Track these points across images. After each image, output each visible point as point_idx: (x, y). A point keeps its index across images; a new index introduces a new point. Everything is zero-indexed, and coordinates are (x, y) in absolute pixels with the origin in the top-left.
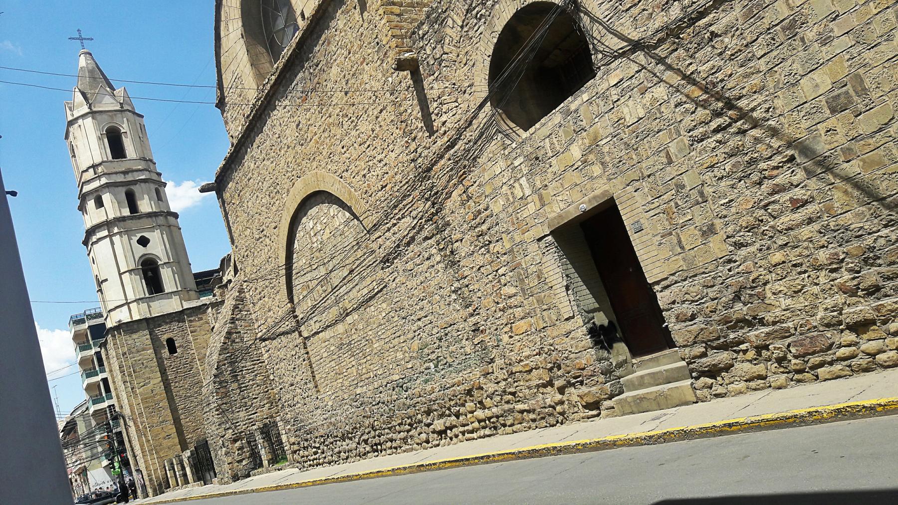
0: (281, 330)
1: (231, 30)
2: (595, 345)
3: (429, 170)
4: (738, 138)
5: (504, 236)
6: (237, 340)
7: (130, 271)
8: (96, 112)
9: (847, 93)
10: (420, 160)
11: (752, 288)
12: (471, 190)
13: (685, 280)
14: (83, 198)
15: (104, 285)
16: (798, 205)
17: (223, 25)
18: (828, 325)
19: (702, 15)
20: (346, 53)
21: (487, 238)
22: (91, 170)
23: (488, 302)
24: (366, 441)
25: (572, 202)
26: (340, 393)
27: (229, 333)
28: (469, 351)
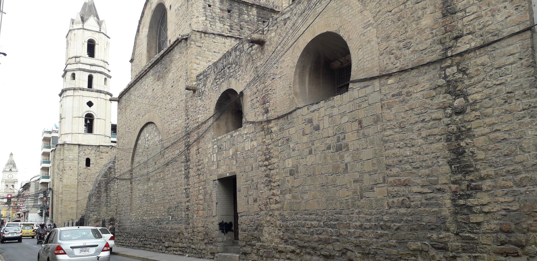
8: (85, 29)
14: (66, 72)
16: (277, 202)
22: (74, 59)
23: (194, 198)
25: (225, 171)
27: (110, 168)
28: (183, 216)
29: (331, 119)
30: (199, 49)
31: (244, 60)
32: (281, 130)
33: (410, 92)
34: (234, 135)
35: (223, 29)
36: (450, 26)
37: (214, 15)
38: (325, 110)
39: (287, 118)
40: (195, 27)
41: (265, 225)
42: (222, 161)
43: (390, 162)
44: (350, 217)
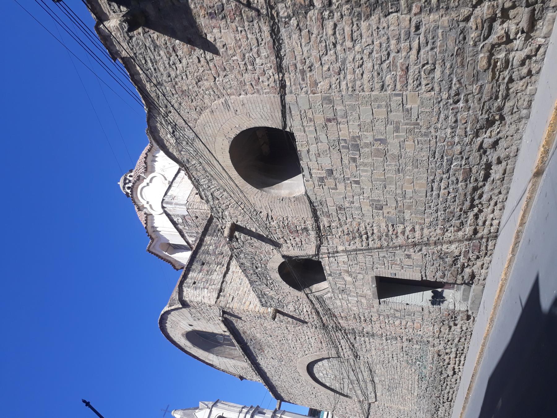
0: (367, 409)
1: (212, 359)
3: (324, 325)
12: (342, 315)
16: (413, 230)
21: (368, 319)
24: (444, 403)
25: (369, 289)
26: (413, 401)
28: (419, 347)
29: (321, 155)
30: (235, 299)
31: (250, 249)
33: (301, 60)
34: (329, 273)
35: (219, 273)
36: (236, 11)
37: (204, 280)
38: (311, 161)
39: (316, 206)
40: (213, 302)
41: (439, 247)
42: (358, 291)
43: (378, 86)
44: (440, 140)
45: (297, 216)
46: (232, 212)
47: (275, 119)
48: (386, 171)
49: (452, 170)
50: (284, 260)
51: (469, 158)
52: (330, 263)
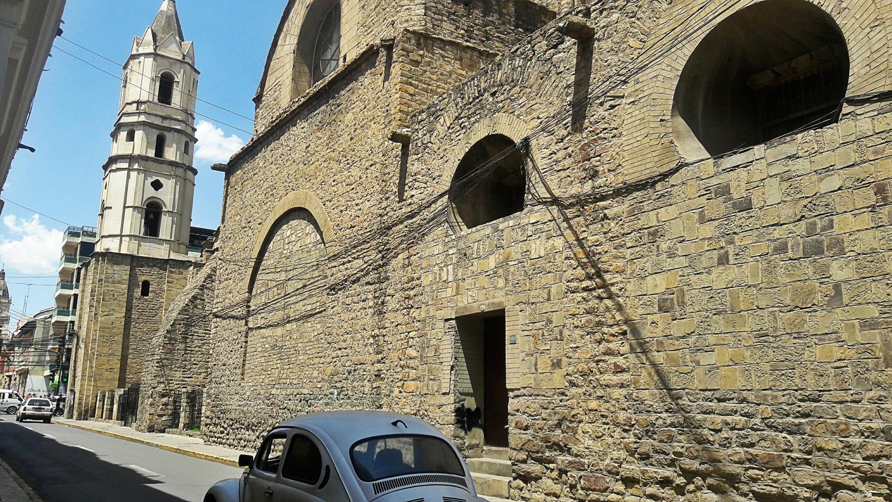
0: (233, 313)
1: (287, 43)
2: (457, 423)
3: (389, 228)
4: (597, 301)
5: (423, 306)
6: (199, 307)
7: (134, 208)
9: (672, 300)
10: (385, 218)
11: (571, 422)
12: (412, 258)
13: (530, 396)
14: (119, 127)
15: (107, 212)
16: (619, 370)
17: (283, 35)
18: (609, 472)
19: (603, 198)
20: (363, 107)
21: (411, 302)
22: (135, 105)
23: (394, 356)
25: (476, 301)
26: (259, 387)
27: (195, 298)
29: (786, 185)
32: (633, 213)
34: (501, 227)
41: (586, 418)
45: (625, 154)
46: (621, 26)
47: (870, 81)
48: (759, 312)
49: (773, 434)
50: (517, 140)
51: (810, 464)
52: (523, 228)
